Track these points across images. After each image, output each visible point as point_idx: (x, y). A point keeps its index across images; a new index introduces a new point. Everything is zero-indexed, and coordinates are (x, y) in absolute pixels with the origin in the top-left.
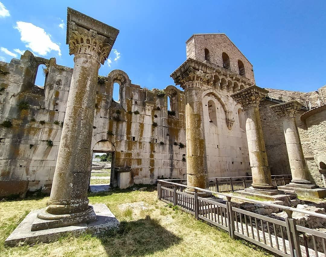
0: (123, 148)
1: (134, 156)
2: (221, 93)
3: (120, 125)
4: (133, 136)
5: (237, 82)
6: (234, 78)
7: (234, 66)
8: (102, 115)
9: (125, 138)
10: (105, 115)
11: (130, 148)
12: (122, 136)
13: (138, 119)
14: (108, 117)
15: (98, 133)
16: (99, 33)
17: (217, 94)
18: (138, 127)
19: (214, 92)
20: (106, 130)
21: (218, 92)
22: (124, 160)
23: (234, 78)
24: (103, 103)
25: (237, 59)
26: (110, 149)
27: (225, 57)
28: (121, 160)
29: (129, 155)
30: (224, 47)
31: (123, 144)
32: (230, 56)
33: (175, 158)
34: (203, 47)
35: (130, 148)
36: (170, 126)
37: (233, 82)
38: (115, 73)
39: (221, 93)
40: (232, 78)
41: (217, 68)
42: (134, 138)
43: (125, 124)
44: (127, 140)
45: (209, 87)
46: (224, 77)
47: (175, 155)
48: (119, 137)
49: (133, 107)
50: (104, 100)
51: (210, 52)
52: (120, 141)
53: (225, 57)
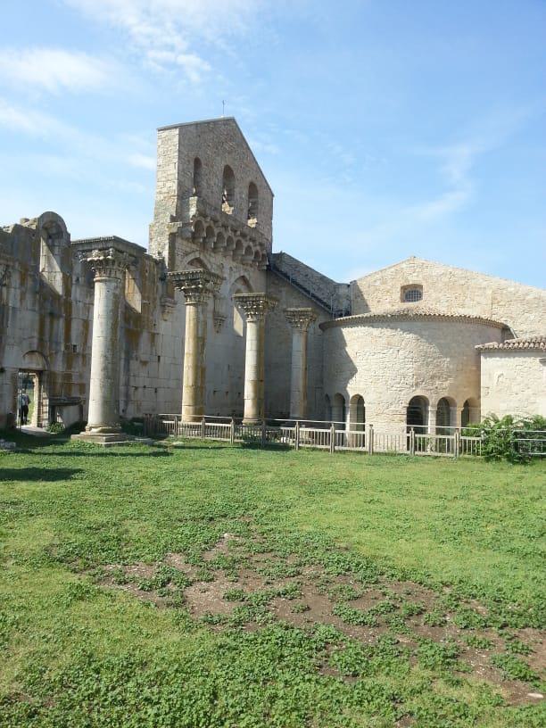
0: (59, 367)
1: (75, 380)
2: (212, 260)
3: (55, 322)
4: (74, 343)
5: (243, 241)
6: (238, 233)
7: (241, 198)
8: (29, 306)
9: (63, 349)
10: (34, 304)
11: (69, 366)
12: (58, 343)
13: (81, 313)
14: (37, 308)
15: (24, 339)
16: (130, 255)
17: (205, 261)
18: (81, 328)
19: (202, 257)
20: (36, 334)
21: (208, 256)
22: (62, 385)
23: (238, 233)
24: (30, 283)
25: (249, 179)
26: (40, 367)
27: (228, 173)
28: (58, 386)
29: (68, 377)
30: (229, 153)
31: (60, 357)
32: (237, 174)
33: (132, 383)
34: (192, 155)
35: (69, 366)
36: (127, 326)
37: (235, 239)
38: (45, 220)
39: (212, 260)
40: (236, 231)
41: (213, 213)
42: (75, 346)
43: (61, 323)
44: (66, 352)
45: (194, 247)
46: (222, 230)
47: (132, 378)
48: (54, 346)
49: (74, 287)
50: (30, 275)
51: (204, 166)
52: (56, 353)
53: (228, 173)
